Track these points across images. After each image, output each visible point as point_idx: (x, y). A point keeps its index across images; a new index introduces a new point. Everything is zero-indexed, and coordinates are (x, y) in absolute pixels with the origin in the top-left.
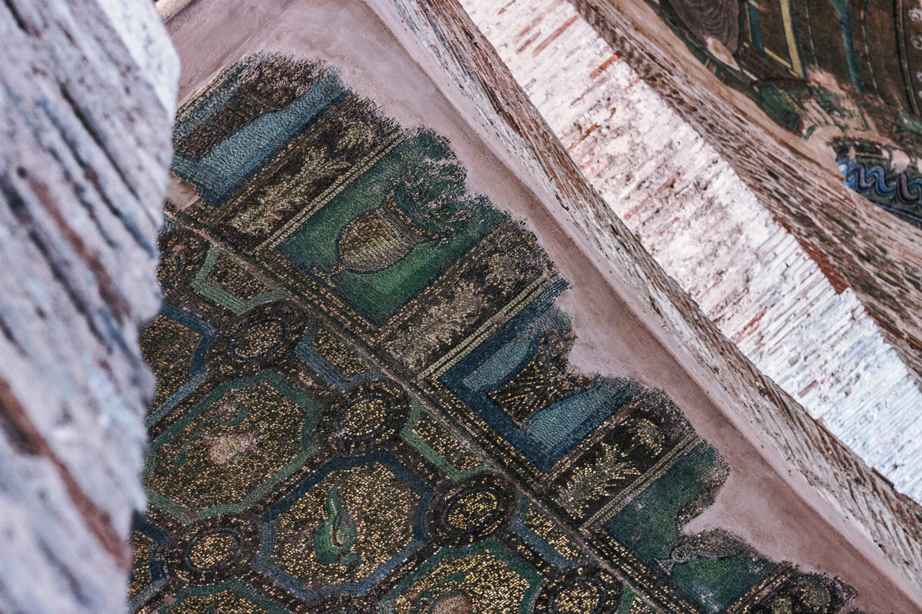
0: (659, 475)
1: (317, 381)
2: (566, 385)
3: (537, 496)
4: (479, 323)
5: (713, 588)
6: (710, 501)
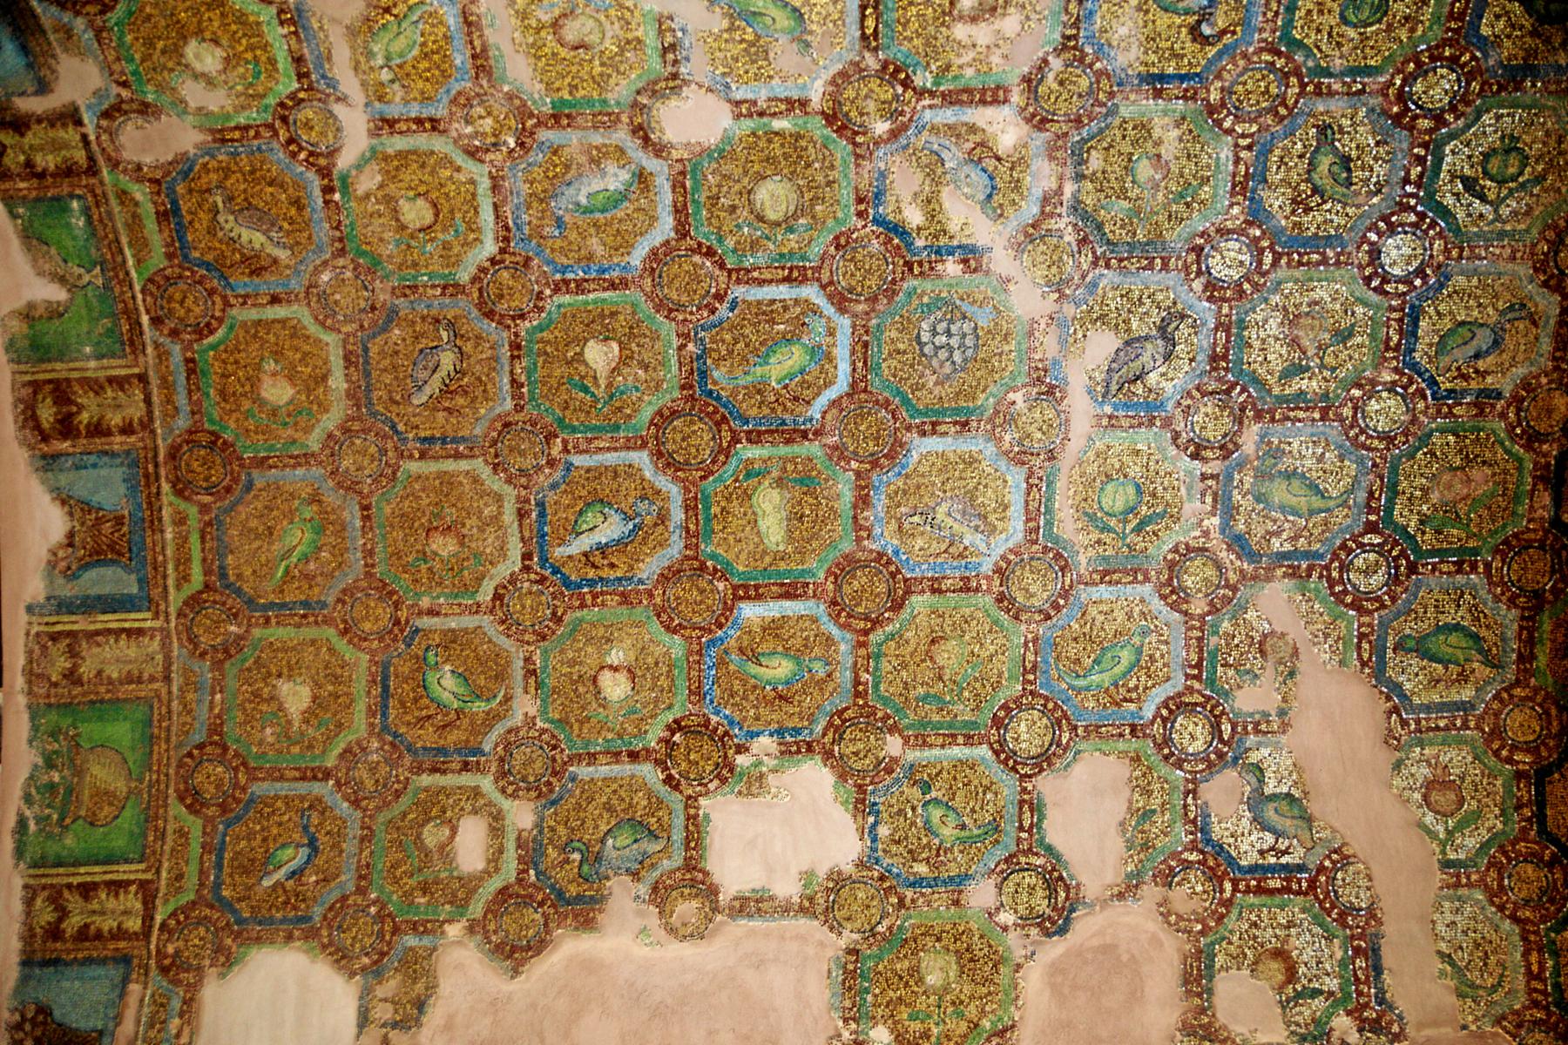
0: (58, 366)
1: (213, 694)
2: (78, 514)
3: (153, 432)
4: (97, 633)
5: (68, 225)
6: (31, 306)
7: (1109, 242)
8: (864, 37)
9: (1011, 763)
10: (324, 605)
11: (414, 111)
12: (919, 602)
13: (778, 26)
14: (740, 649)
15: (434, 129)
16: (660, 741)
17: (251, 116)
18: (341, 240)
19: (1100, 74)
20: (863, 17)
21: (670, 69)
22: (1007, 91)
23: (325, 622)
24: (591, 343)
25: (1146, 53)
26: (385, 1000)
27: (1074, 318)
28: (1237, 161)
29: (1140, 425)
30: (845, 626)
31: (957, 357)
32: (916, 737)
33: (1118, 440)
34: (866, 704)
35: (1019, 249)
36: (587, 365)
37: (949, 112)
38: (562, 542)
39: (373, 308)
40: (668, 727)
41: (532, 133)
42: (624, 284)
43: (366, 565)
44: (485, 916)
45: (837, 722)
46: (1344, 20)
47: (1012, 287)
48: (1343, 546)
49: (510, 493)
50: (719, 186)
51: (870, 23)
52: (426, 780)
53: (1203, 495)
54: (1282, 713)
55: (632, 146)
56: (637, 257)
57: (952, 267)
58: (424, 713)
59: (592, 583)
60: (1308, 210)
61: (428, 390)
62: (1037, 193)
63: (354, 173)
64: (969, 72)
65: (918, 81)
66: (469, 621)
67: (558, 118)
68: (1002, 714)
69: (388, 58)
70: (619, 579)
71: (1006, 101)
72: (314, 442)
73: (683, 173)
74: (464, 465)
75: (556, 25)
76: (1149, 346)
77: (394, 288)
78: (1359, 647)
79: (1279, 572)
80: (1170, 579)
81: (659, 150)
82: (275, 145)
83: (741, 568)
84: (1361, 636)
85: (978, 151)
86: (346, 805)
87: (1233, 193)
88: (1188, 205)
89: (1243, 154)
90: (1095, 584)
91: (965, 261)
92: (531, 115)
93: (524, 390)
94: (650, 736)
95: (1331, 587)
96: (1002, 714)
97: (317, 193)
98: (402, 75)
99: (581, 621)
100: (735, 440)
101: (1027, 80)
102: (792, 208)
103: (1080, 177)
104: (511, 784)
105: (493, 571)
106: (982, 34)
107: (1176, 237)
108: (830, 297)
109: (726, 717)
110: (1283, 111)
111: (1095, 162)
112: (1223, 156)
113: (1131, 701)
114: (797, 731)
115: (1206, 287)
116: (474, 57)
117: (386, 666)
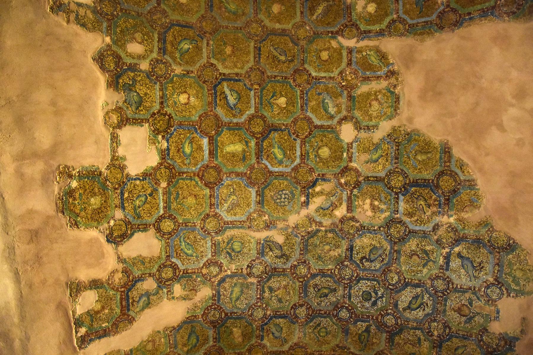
7: (308, 240)
8: (368, 177)
9: (158, 220)
10: (212, 11)
11: (354, 59)
12: (207, 191)
13: (373, 156)
14: (194, 137)
15: (348, 64)
16: (166, 112)
17: (354, 17)
18: (318, 34)
19: (354, 236)
20: (374, 177)
21: (363, 127)
22: (351, 213)
23: (206, 11)
24: (286, 99)
25: (359, 246)
26: (86, 13)
27: (288, 231)
28: (328, 270)
29: (258, 251)
30: (200, 170)
31: (278, 201)
32: (166, 191)
33: (253, 245)
34: (176, 176)
35: (307, 216)
36: (280, 98)
37: (346, 198)
38: (228, 86)
39: (298, 39)
40: (170, 114)
41: (346, 90)
42: (302, 110)
43: (223, 26)
44: (112, 51)
45: (171, 167)
46: (364, 292)
47: (297, 215)
48: (221, 308)
49: (243, 72)
50: (328, 138)
51: (372, 179)
52: (156, 36)
53: (237, 269)
54: (173, 298)
55: (341, 116)
56: (309, 114)
57: (303, 199)
58: (177, 37)
59: (215, 93)
60: (314, 288)
61: (274, 51)
62: (323, 221)
63: (337, 40)
64: (357, 203)
65: (355, 190)
66: (205, 55)
67: (351, 98)
68: (173, 217)
69: (369, 55)
70: (216, 102)
71: (348, 212)
72: (261, 16)
73: (332, 128)
74: (252, 59)
75: (377, 99)
76: (279, 252)
77: (304, 46)
78: (192, 316)
79: (214, 292)
80: (213, 262)
81: (340, 123)
82: (345, 21)
83: (219, 138)
84: (195, 316)
85: (335, 205)
86: (149, 9)
87: (319, 270)
88: (317, 259)
89: (329, 272)
90: (212, 241)
91: (304, 202)
92: (351, 90)
93: (273, 79)
94: (168, 109)
95: (210, 306)
96: (173, 217)
97: (332, 30)
98: (365, 58)
99: (204, 90)
100: (257, 138)
101: (354, 217)
102: (322, 157)
103: (326, 231)
104: (154, 64)
105: (220, 64)
106: (367, 206)
107: (309, 256)
108: (296, 166)
109: (173, 133)
110: (340, 279)
111: (330, 235)
112: (330, 266)
113: (177, 255)
114: (168, 155)
115: (295, 266)
116: (368, 77)
117: (191, 27)
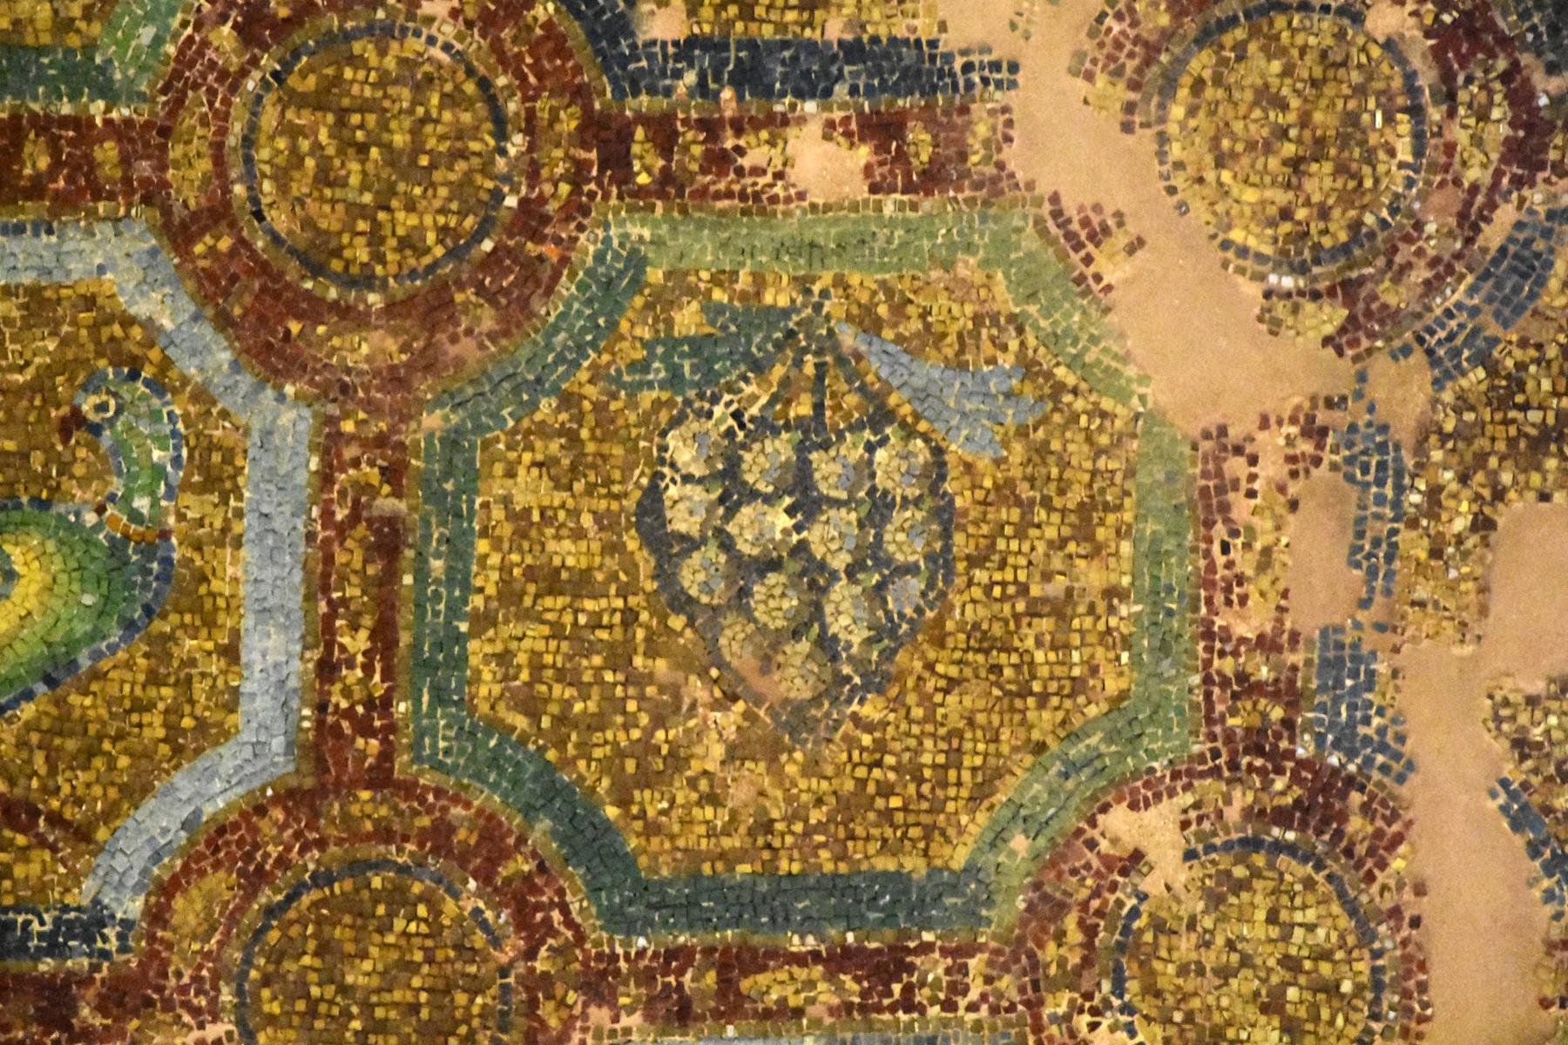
27: (1427, 431)
47: (1112, 267)
